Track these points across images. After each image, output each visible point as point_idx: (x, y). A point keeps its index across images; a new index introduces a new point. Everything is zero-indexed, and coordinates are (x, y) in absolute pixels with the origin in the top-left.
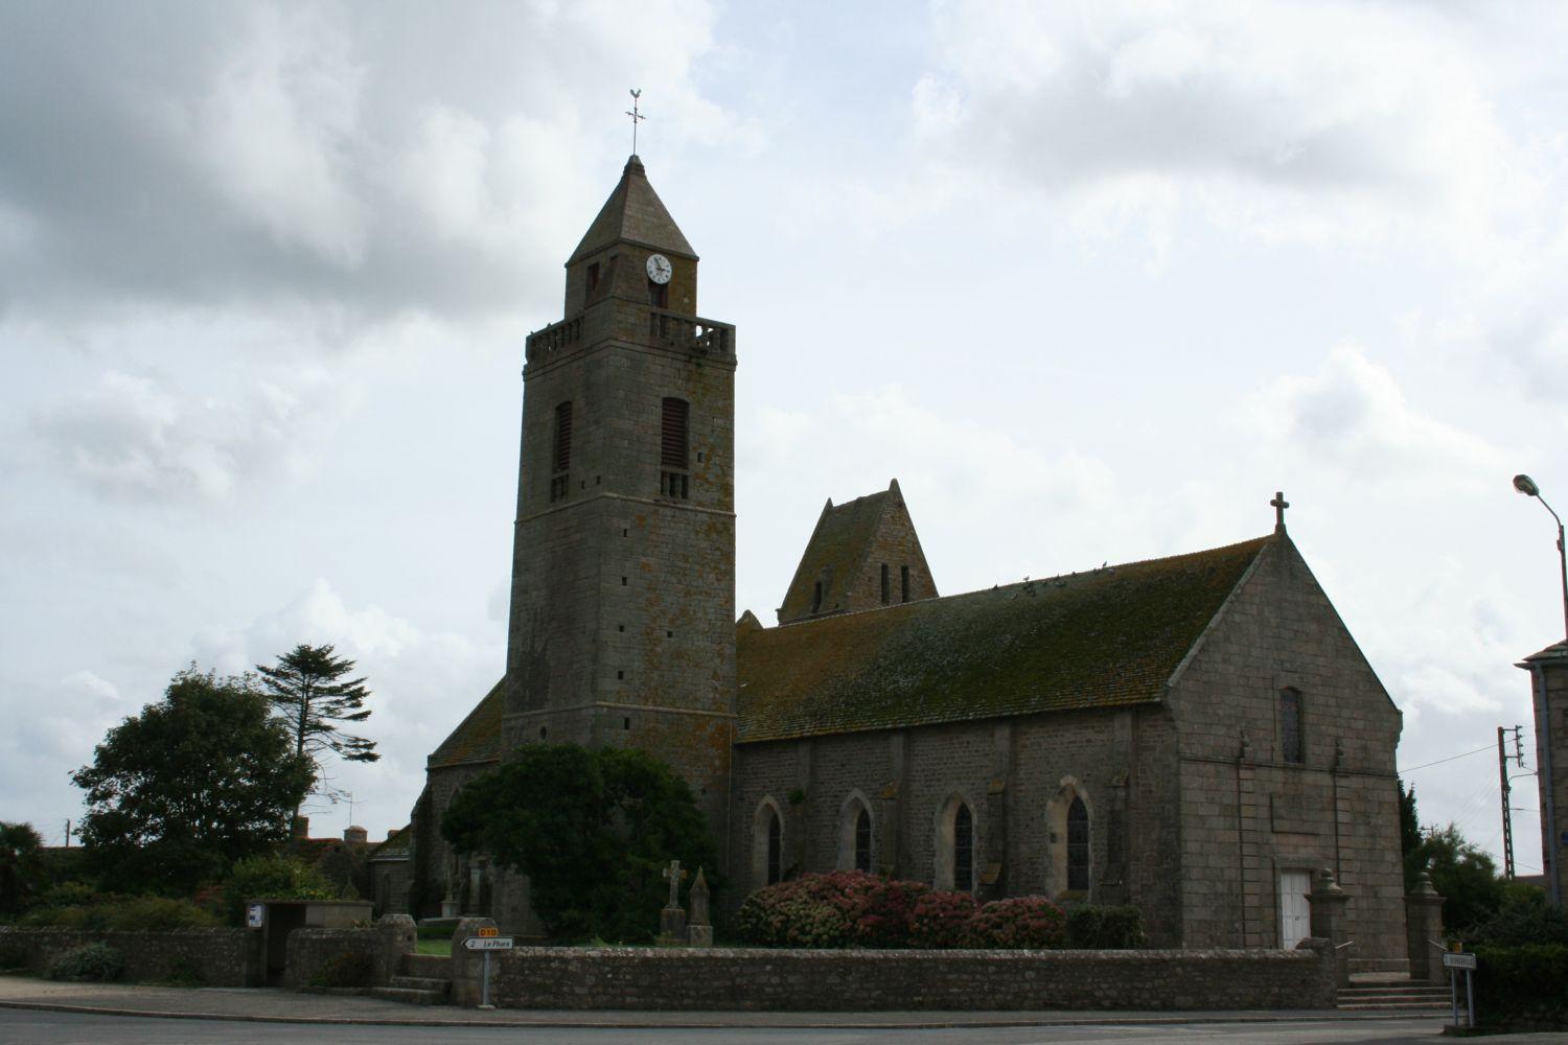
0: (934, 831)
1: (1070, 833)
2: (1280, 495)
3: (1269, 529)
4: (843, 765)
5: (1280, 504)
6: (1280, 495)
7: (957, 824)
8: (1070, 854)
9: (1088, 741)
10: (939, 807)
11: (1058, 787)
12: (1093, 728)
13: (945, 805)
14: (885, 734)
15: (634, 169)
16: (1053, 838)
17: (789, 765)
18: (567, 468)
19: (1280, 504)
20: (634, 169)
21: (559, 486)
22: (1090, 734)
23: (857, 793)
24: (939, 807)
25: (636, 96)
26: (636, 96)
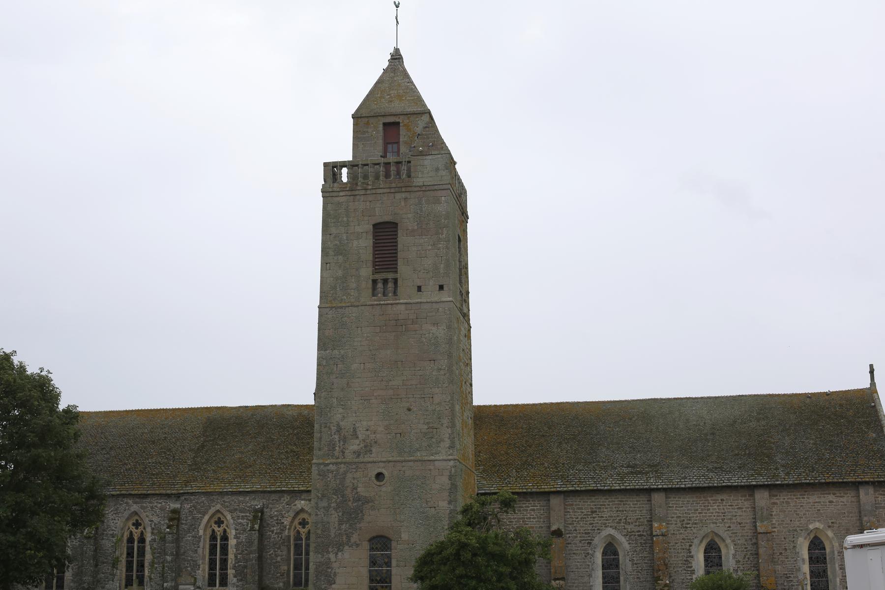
0: (692, 557)
1: (810, 558)
2: (871, 366)
3: (866, 384)
4: (592, 512)
5: (872, 372)
6: (871, 366)
7: (705, 553)
8: (811, 572)
9: (830, 502)
10: (696, 541)
11: (807, 530)
12: (834, 494)
13: (701, 542)
14: (650, 491)
15: (396, 58)
16: (803, 560)
17: (533, 510)
18: (396, 272)
19: (872, 372)
20: (396, 58)
21: (380, 285)
22: (831, 497)
23: (612, 532)
24: (696, 541)
25: (397, 7)
26: (397, 7)
